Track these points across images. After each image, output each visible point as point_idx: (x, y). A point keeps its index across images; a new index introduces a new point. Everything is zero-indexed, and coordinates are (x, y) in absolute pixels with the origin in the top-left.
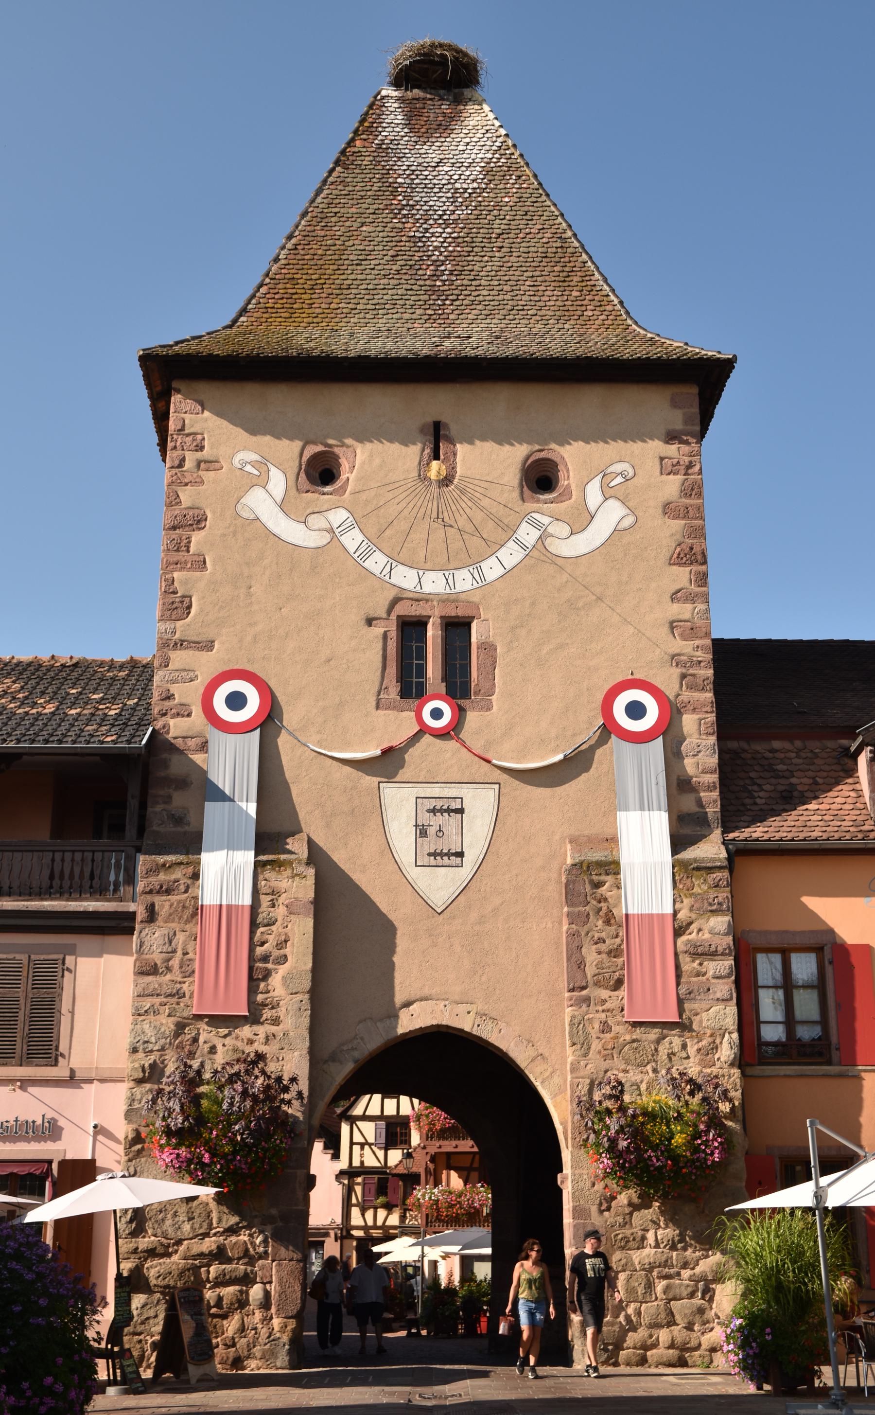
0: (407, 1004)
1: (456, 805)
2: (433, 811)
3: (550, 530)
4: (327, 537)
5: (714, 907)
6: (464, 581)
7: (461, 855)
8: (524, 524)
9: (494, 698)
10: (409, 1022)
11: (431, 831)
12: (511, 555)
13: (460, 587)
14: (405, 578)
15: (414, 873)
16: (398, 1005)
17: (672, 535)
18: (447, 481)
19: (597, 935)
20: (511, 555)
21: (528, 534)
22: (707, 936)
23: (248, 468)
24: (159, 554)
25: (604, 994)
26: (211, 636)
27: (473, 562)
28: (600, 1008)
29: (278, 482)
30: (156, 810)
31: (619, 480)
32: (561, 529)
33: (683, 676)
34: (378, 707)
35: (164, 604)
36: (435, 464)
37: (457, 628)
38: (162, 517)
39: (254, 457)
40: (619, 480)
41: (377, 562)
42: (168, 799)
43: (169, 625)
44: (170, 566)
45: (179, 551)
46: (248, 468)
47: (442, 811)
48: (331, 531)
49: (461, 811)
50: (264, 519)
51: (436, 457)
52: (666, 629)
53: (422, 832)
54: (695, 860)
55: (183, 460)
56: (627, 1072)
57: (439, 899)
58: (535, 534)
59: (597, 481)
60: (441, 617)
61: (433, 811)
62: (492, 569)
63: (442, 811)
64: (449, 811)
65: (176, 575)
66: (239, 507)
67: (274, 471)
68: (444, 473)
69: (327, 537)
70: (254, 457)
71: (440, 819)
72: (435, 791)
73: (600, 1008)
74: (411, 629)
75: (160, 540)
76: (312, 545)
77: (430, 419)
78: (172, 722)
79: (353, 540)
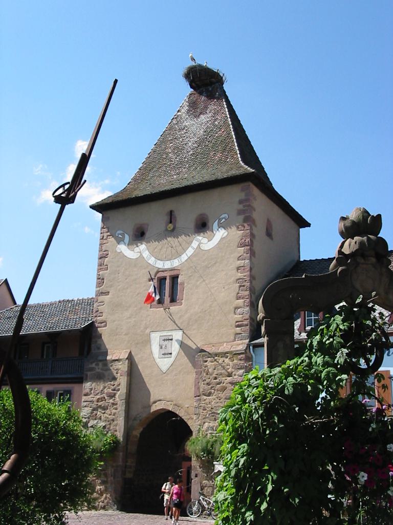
0: (155, 402)
1: (170, 338)
2: (164, 340)
3: (202, 241)
4: (139, 254)
5: (240, 367)
6: (176, 263)
7: (171, 354)
8: (194, 241)
9: (183, 301)
10: (154, 408)
11: (164, 347)
12: (190, 252)
13: (174, 266)
14: (160, 265)
15: (158, 360)
16: (152, 400)
17: (239, 237)
18: (173, 230)
19: (204, 378)
20: (190, 252)
21: (195, 244)
22: (237, 377)
23: (120, 236)
24: (96, 267)
25: (205, 397)
26: (109, 291)
27: (179, 255)
28: (204, 402)
29: (127, 238)
30: (93, 346)
31: (224, 220)
32: (205, 240)
33: (240, 286)
34: (151, 308)
35: (97, 282)
36: (170, 224)
37: (175, 278)
38: (96, 255)
39: (122, 232)
40: (224, 220)
41: (152, 260)
42: (96, 342)
43: (98, 289)
44: (99, 270)
45: (101, 266)
46: (120, 236)
47: (167, 340)
48: (140, 252)
49: (172, 340)
50: (123, 252)
51: (171, 222)
52: (235, 270)
53: (161, 348)
54: (235, 351)
55: (103, 237)
56: (210, 423)
57: (164, 369)
58: (198, 243)
59: (217, 221)
60: (170, 276)
61: (164, 340)
62: (184, 257)
63: (167, 340)
64: (168, 340)
65: (101, 273)
66: (117, 249)
67: (126, 234)
68: (172, 227)
69: (139, 254)
70: (122, 232)
71: (166, 342)
72: (165, 333)
73: (204, 402)
74: (162, 280)
75: (95, 262)
76: (135, 258)
77: (169, 210)
78: (98, 318)
79: (146, 254)
